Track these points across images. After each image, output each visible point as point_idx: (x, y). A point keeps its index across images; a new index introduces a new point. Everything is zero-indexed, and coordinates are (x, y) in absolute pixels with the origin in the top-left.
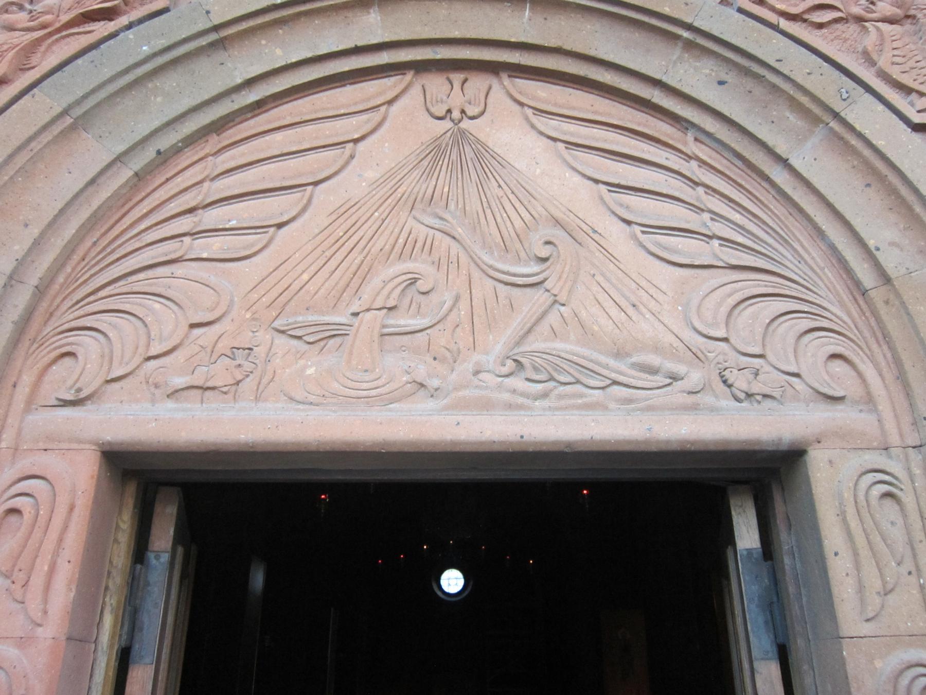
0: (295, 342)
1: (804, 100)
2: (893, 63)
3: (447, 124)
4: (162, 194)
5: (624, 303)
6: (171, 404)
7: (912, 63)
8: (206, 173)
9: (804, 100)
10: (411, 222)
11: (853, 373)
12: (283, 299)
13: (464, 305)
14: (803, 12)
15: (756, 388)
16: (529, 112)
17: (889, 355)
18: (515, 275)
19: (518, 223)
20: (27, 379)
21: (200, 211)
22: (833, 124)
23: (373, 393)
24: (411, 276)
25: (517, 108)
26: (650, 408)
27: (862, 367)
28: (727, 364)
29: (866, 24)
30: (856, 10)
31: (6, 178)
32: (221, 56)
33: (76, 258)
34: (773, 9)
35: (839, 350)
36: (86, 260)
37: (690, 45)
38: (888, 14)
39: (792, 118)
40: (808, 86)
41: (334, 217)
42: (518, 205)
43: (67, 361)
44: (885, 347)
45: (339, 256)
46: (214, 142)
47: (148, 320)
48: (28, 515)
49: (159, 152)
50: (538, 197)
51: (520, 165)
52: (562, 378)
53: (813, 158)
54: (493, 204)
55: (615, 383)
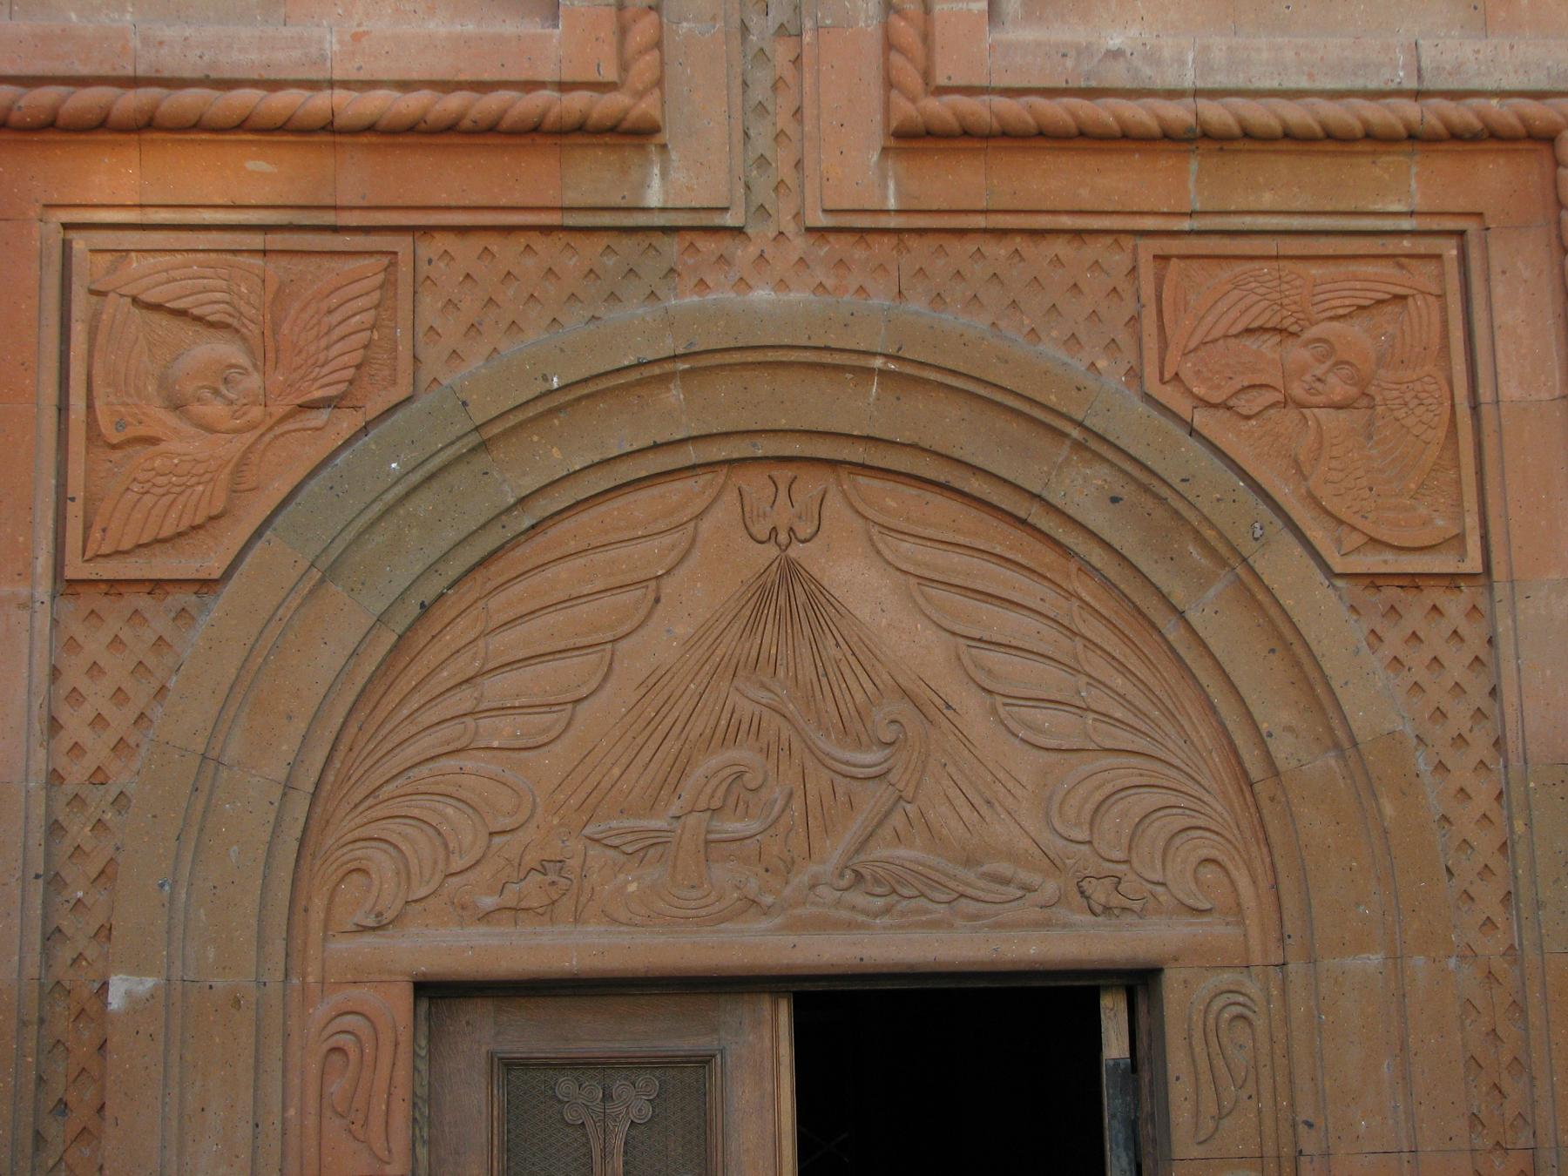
0: (612, 853)
3: (772, 551)
4: (430, 658)
5: (977, 801)
6: (482, 929)
8: (479, 628)
10: (735, 697)
11: (1226, 880)
12: (592, 800)
13: (797, 804)
14: (1230, 397)
15: (1116, 900)
16: (875, 530)
17: (1268, 860)
18: (855, 766)
19: (859, 697)
20: (318, 903)
21: (478, 680)
22: (1240, 570)
23: (703, 912)
24: (736, 769)
25: (861, 521)
26: (1000, 926)
27: (1235, 873)
28: (1087, 873)
30: (1297, 391)
31: (260, 660)
32: (481, 461)
33: (343, 748)
35: (1214, 853)
36: (356, 751)
37: (1079, 446)
41: (643, 690)
42: (859, 671)
43: (355, 876)
44: (1265, 850)
45: (652, 745)
46: (479, 576)
47: (444, 828)
48: (353, 1055)
49: (422, 605)
50: (883, 658)
51: (863, 612)
52: (906, 892)
53: (1213, 614)
54: (830, 670)
55: (962, 895)
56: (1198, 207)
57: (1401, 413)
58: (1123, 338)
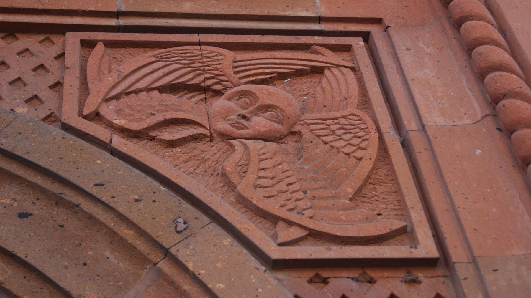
1: (127, 233)
2: (256, 187)
7: (282, 186)
9: (127, 233)
22: (164, 265)
29: (234, 142)
30: (223, 126)
34: (110, 125)
38: (263, 130)
39: (114, 259)
40: (132, 216)
56: (124, 9)
57: (330, 138)
58: (45, 94)
